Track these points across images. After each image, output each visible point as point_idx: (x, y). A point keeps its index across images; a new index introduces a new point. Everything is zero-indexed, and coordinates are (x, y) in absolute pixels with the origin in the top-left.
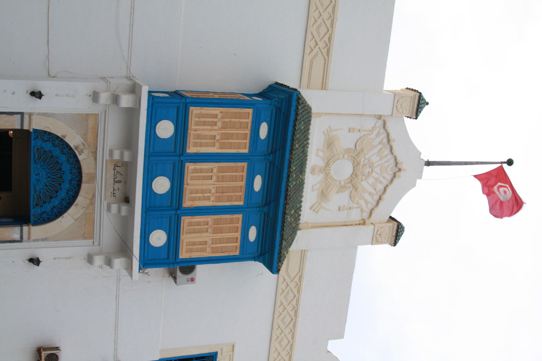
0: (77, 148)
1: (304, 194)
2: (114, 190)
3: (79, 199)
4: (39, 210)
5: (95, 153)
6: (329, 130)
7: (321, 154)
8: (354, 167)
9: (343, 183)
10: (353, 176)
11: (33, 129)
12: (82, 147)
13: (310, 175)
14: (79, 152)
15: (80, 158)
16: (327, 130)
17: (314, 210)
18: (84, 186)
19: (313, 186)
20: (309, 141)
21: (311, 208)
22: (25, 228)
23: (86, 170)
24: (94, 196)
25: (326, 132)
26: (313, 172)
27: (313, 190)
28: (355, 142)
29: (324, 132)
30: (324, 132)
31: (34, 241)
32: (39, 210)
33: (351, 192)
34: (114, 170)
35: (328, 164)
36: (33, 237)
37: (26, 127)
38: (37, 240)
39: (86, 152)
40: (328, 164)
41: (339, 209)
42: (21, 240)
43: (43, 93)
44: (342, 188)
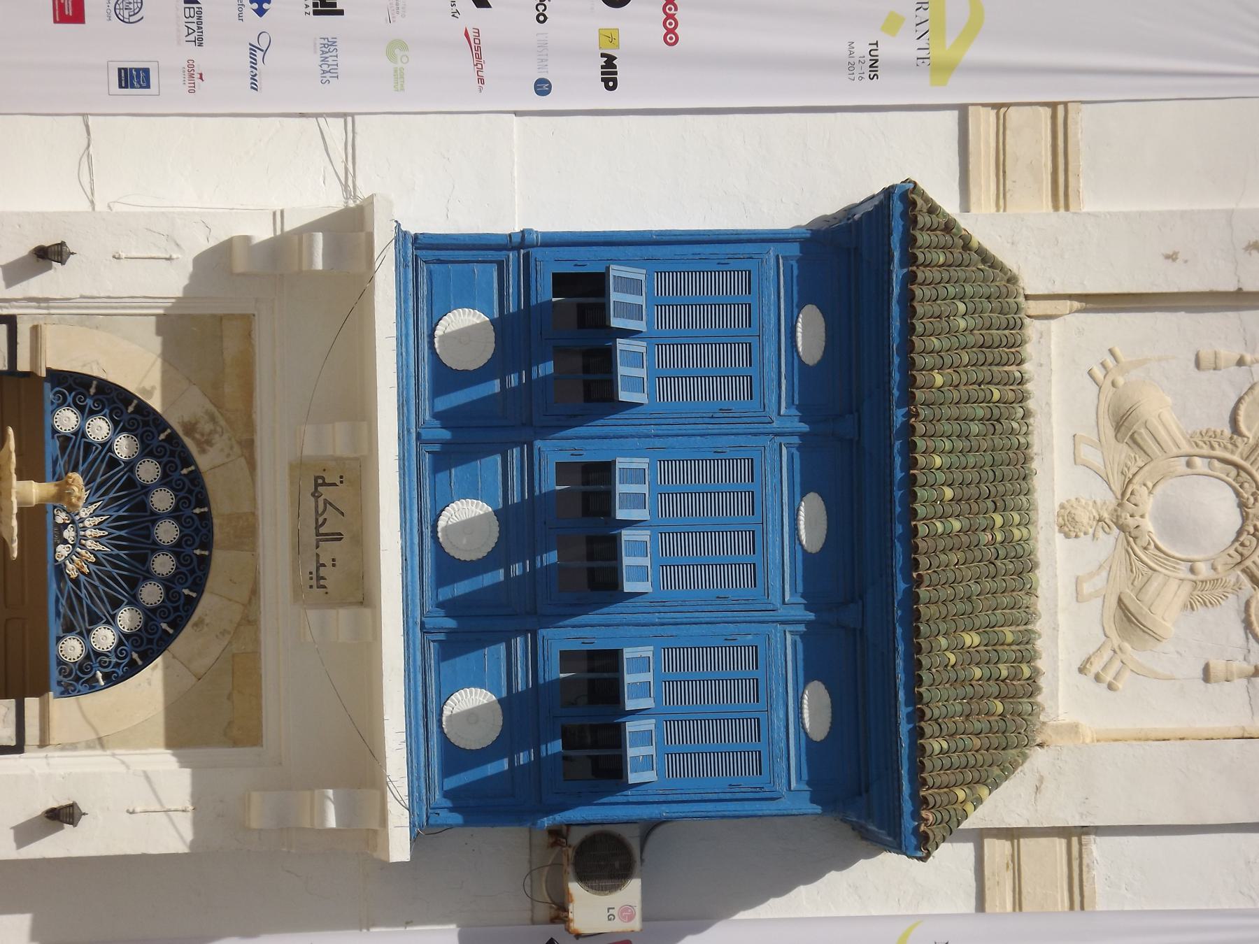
0: (190, 428)
1: (1041, 605)
2: (320, 566)
3: (208, 605)
4: (72, 649)
5: (248, 446)
6: (1110, 362)
7: (1093, 456)
8: (1242, 505)
9: (1204, 570)
10: (1244, 537)
11: (49, 370)
12: (208, 427)
13: (1059, 537)
14: (199, 444)
15: (204, 462)
16: (1103, 365)
17: (1097, 678)
18: (220, 558)
19: (1078, 582)
20: (1031, 404)
21: (1082, 670)
22: (32, 704)
23: (221, 505)
24: (255, 592)
25: (1099, 373)
26: (1068, 525)
27: (1079, 597)
28: (1232, 404)
29: (1090, 373)
30: (1090, 373)
31: (63, 747)
32: (72, 649)
33: (1248, 604)
34: (316, 495)
35: (1125, 495)
36: (56, 735)
37: (23, 365)
38: (73, 746)
39: (220, 442)
40: (1125, 495)
41: (1207, 675)
42: (18, 748)
43: (71, 246)
44: (1202, 594)
